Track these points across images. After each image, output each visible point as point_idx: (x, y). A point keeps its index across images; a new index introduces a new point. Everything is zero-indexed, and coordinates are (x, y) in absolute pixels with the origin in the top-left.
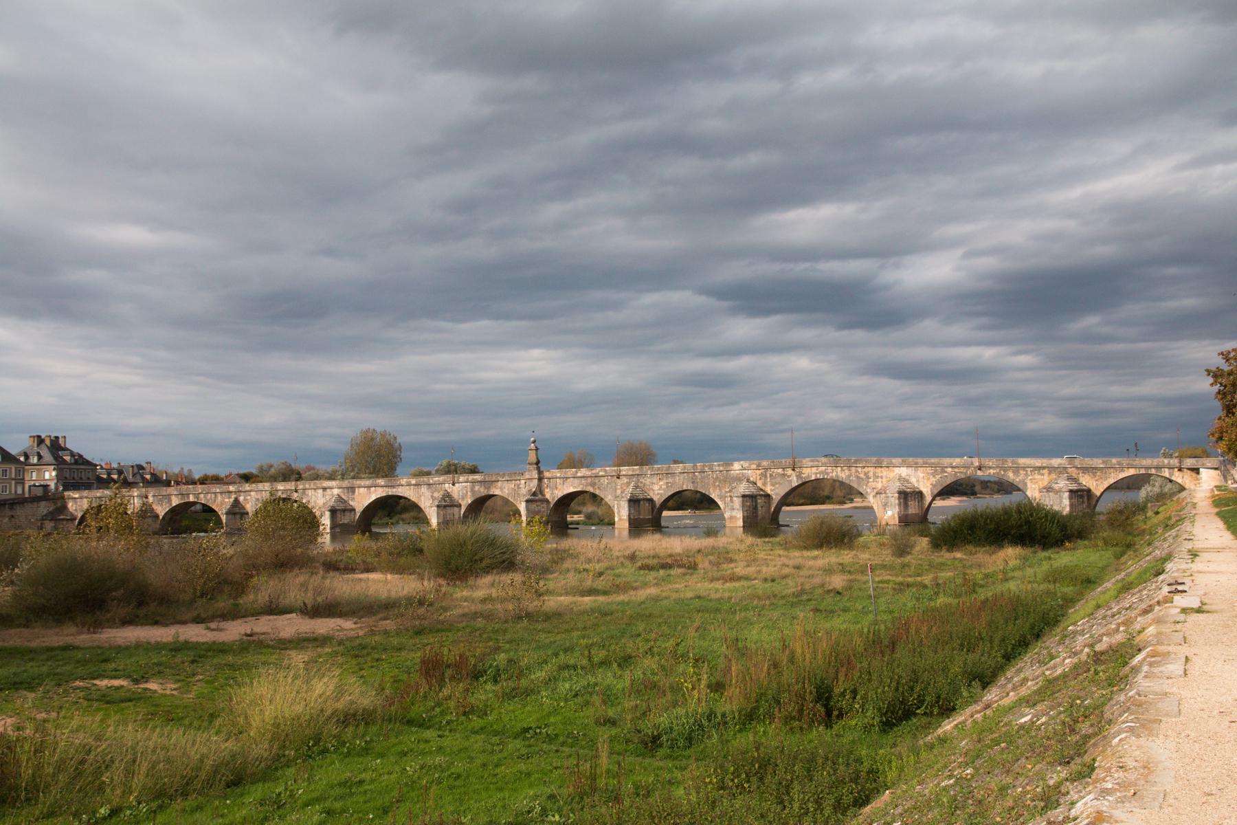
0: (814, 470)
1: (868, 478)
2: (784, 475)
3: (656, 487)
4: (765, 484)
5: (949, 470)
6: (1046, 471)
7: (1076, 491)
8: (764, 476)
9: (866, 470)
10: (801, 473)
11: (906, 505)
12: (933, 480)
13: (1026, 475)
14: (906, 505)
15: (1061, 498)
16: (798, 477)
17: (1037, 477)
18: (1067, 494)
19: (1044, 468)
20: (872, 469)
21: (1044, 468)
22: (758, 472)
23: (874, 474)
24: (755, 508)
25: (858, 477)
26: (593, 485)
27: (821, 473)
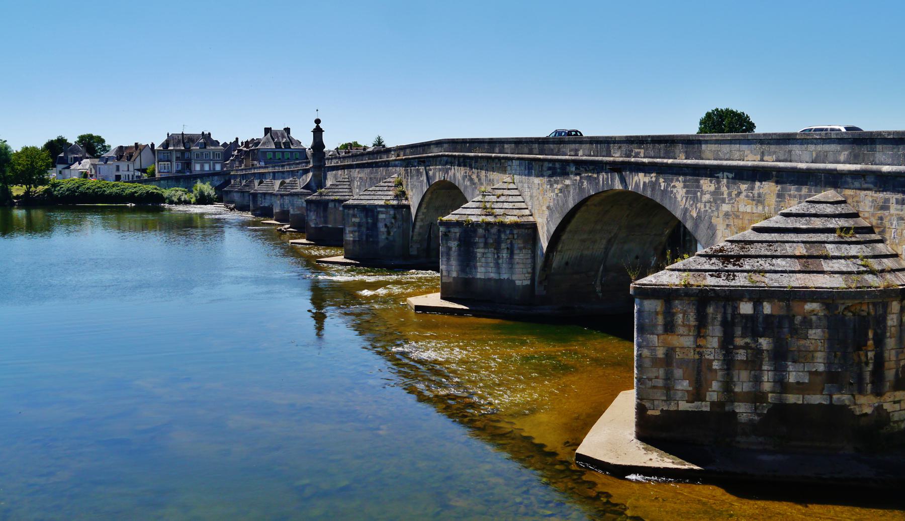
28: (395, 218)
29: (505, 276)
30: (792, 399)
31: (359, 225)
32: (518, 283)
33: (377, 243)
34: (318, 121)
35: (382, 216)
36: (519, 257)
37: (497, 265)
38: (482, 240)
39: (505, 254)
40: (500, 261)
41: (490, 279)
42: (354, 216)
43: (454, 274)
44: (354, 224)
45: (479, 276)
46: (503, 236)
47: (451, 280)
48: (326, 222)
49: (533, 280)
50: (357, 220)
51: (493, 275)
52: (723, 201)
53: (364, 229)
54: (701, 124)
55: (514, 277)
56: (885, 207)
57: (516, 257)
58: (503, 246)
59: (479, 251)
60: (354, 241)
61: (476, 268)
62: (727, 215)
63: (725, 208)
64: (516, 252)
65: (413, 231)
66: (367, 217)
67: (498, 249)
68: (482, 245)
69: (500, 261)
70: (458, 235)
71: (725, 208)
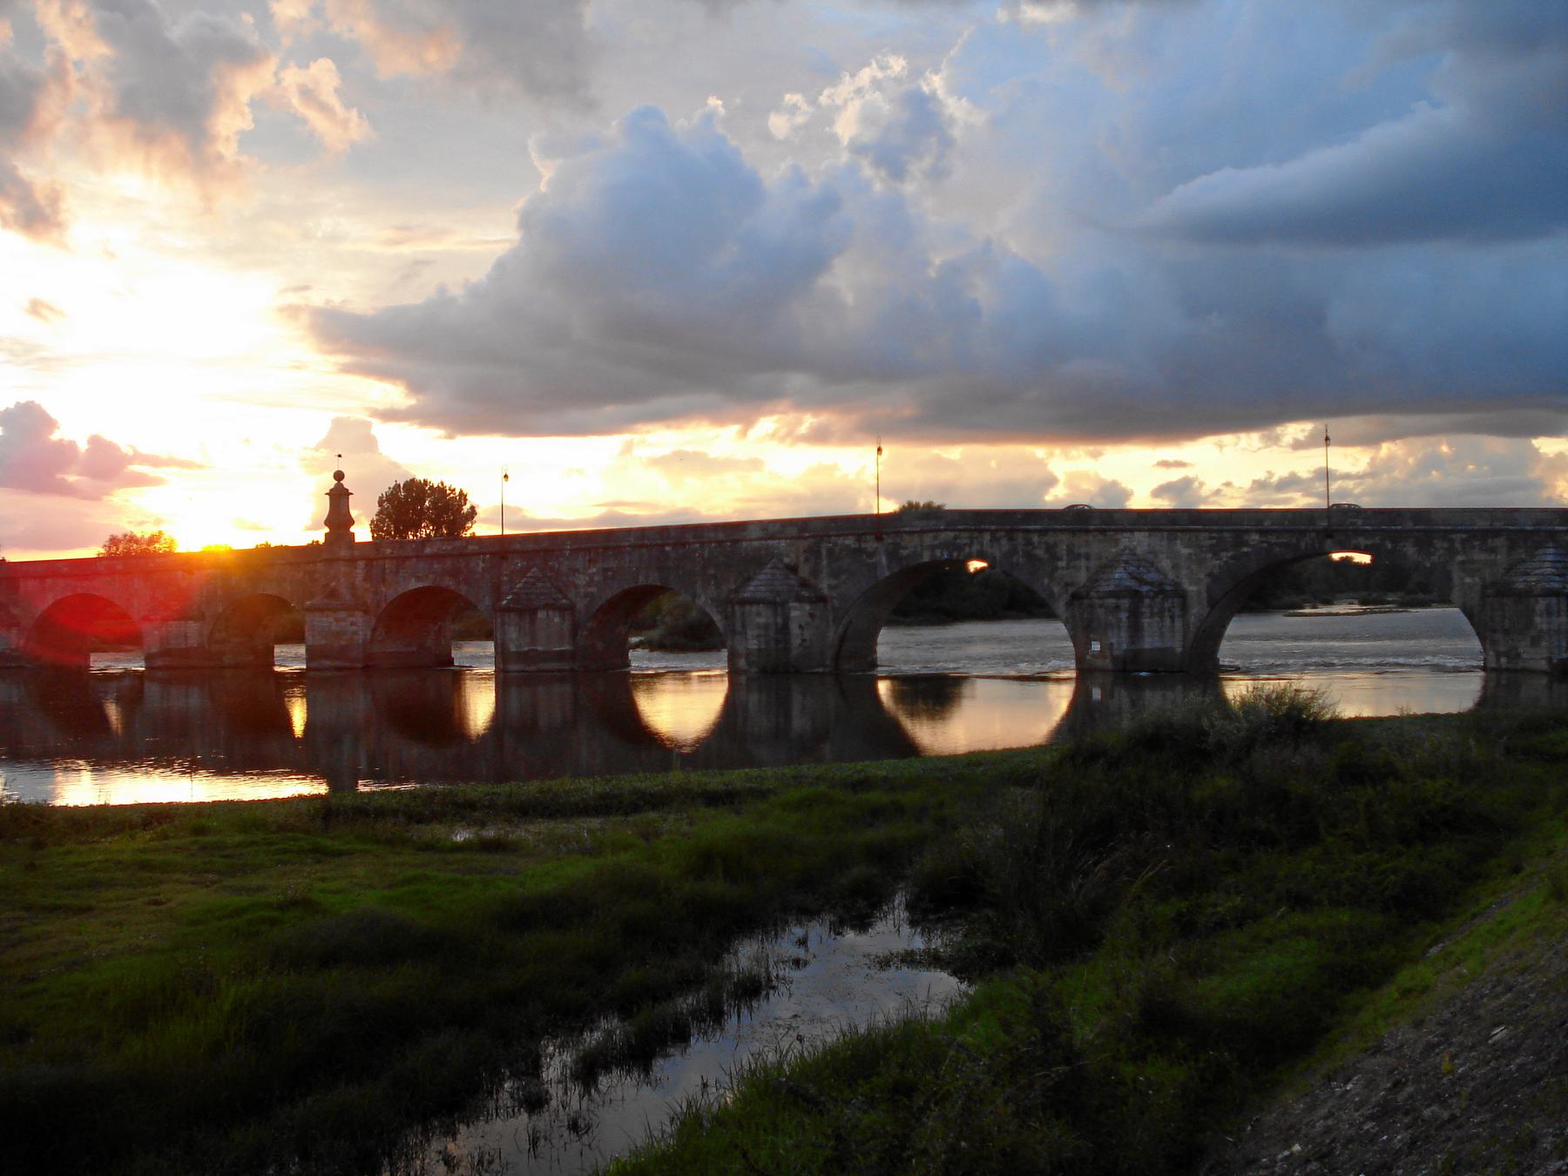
0: (928, 539)
1: (1055, 557)
2: (859, 551)
3: (581, 580)
4: (815, 572)
5: (1255, 537)
6: (1500, 542)
8: (814, 552)
9: (1050, 539)
13: (1452, 552)
16: (893, 554)
19: (1496, 533)
20: (1064, 537)
21: (1496, 533)
22: (803, 544)
23: (1070, 550)
24: (784, 629)
25: (1029, 556)
26: (454, 573)
27: (943, 546)
28: (811, 615)
31: (766, 627)
33: (787, 650)
34: (339, 476)
35: (794, 613)
37: (1162, 635)
39: (1168, 621)
42: (759, 614)
43: (1125, 646)
44: (759, 627)
45: (1147, 646)
48: (534, 641)
50: (761, 620)
51: (1158, 645)
52: (1458, 553)
53: (772, 633)
54: (380, 503)
59: (1146, 621)
60: (759, 650)
62: (1463, 563)
63: (1460, 558)
66: (775, 613)
67: (1162, 618)
71: (1460, 558)
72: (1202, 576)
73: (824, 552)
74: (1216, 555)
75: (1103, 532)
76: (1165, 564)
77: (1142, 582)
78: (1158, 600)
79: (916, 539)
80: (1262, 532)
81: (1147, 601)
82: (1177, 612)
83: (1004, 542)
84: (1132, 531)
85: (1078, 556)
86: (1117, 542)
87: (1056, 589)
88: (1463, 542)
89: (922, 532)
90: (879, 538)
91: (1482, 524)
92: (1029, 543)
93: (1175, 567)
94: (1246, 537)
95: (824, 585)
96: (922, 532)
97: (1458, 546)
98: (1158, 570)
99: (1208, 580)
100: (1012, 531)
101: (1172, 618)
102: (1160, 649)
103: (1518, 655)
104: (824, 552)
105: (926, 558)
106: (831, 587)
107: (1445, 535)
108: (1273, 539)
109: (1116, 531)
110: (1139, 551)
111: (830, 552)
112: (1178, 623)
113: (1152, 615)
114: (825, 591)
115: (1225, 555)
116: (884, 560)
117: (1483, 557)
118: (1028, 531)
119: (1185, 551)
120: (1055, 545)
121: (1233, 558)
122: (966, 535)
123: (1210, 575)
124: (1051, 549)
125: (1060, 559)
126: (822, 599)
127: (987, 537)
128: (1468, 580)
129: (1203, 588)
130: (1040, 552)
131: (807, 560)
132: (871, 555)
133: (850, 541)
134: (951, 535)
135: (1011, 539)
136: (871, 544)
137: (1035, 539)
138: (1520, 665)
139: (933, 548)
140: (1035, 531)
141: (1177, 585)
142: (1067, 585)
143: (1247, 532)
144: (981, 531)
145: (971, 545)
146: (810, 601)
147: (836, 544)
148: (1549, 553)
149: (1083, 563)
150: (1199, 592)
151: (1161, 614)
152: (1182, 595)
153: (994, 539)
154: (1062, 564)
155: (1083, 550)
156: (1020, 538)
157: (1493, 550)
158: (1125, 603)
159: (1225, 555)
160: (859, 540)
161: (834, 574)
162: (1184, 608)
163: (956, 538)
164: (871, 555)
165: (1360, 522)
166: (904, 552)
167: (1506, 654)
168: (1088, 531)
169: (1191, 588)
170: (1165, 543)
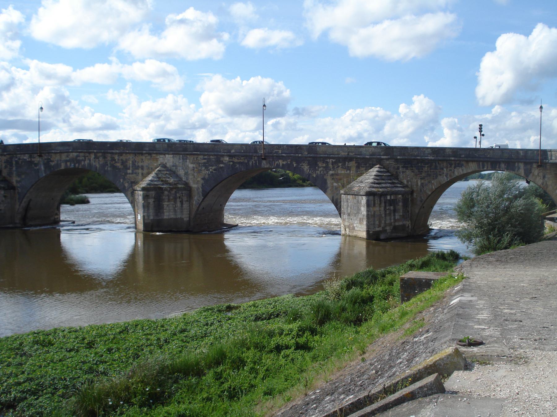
0: (64, 157)
2: (31, 163)
4: (10, 174)
5: (227, 159)
6: (353, 164)
7: (383, 194)
8: (9, 163)
9: (124, 157)
10: (49, 161)
11: (159, 208)
12: (205, 173)
13: (327, 168)
14: (159, 208)
15: (359, 202)
16: (47, 165)
17: (341, 171)
18: (364, 200)
20: (131, 157)
21: (351, 159)
23: (134, 163)
25: (113, 167)
27: (72, 160)
28: (5, 197)
29: (179, 216)
30: (397, 224)
32: (185, 219)
36: (186, 205)
37: (175, 211)
38: (167, 197)
39: (179, 204)
40: (176, 209)
41: (171, 219)
43: (152, 218)
45: (165, 217)
46: (178, 195)
47: (149, 221)
49: (190, 217)
51: (172, 216)
52: (330, 170)
55: (184, 216)
56: (398, 168)
57: (184, 206)
58: (178, 200)
59: (165, 204)
61: (163, 213)
62: (332, 175)
63: (331, 172)
64: (184, 203)
65: (20, 205)
67: (175, 202)
68: (167, 200)
69: (176, 209)
70: (153, 195)
71: (331, 172)
72: (199, 179)
73: (14, 163)
74: (207, 168)
75: (150, 154)
76: (181, 172)
77: (166, 182)
78: (173, 192)
79: (58, 157)
80: (231, 156)
81: (166, 193)
82: (185, 199)
83: (101, 159)
84: (165, 154)
85: (137, 168)
86: (157, 160)
87: (126, 185)
88: (333, 163)
89: (61, 153)
90: (40, 156)
91: (343, 154)
92: (113, 159)
93: (186, 174)
94: (222, 159)
95: (14, 180)
96: (61, 153)
97: (331, 166)
98: (177, 176)
99: (202, 182)
100: (104, 153)
101: (182, 202)
102: (176, 219)
103: (354, 228)
104: (14, 163)
105: (63, 167)
106: (17, 182)
107: (324, 160)
108: (236, 160)
109: (156, 154)
110: (168, 165)
111: (17, 162)
112: (186, 205)
113: (169, 200)
114: (15, 183)
115: (211, 169)
116: (42, 168)
117: (343, 172)
118: (112, 153)
119: (191, 166)
120: (127, 161)
121: (215, 170)
122: (82, 154)
123: (203, 179)
124: (124, 163)
125: (129, 169)
126: (13, 188)
127: (93, 156)
128: (335, 184)
129: (200, 185)
130: (119, 165)
131: (6, 167)
132: (36, 165)
133: (26, 157)
134: (75, 154)
135: (105, 157)
136: (37, 159)
137: (116, 157)
138: (355, 234)
139: (66, 161)
140: (116, 153)
141: (186, 184)
142: (132, 183)
143: (223, 156)
144: (90, 153)
145: (84, 161)
146: (4, 189)
147: (19, 159)
148: (374, 171)
149: (140, 171)
150: (198, 189)
151: (175, 199)
152: (188, 189)
153: (96, 157)
154: (130, 171)
155: (140, 164)
156: (109, 157)
157: (349, 168)
158: (153, 193)
159: (211, 169)
160: (31, 157)
161: (19, 175)
162: (190, 196)
163: (77, 156)
164: (36, 165)
165: (280, 151)
166: (52, 164)
167: (349, 227)
168: (142, 154)
169: (194, 186)
170: (181, 161)
